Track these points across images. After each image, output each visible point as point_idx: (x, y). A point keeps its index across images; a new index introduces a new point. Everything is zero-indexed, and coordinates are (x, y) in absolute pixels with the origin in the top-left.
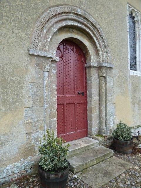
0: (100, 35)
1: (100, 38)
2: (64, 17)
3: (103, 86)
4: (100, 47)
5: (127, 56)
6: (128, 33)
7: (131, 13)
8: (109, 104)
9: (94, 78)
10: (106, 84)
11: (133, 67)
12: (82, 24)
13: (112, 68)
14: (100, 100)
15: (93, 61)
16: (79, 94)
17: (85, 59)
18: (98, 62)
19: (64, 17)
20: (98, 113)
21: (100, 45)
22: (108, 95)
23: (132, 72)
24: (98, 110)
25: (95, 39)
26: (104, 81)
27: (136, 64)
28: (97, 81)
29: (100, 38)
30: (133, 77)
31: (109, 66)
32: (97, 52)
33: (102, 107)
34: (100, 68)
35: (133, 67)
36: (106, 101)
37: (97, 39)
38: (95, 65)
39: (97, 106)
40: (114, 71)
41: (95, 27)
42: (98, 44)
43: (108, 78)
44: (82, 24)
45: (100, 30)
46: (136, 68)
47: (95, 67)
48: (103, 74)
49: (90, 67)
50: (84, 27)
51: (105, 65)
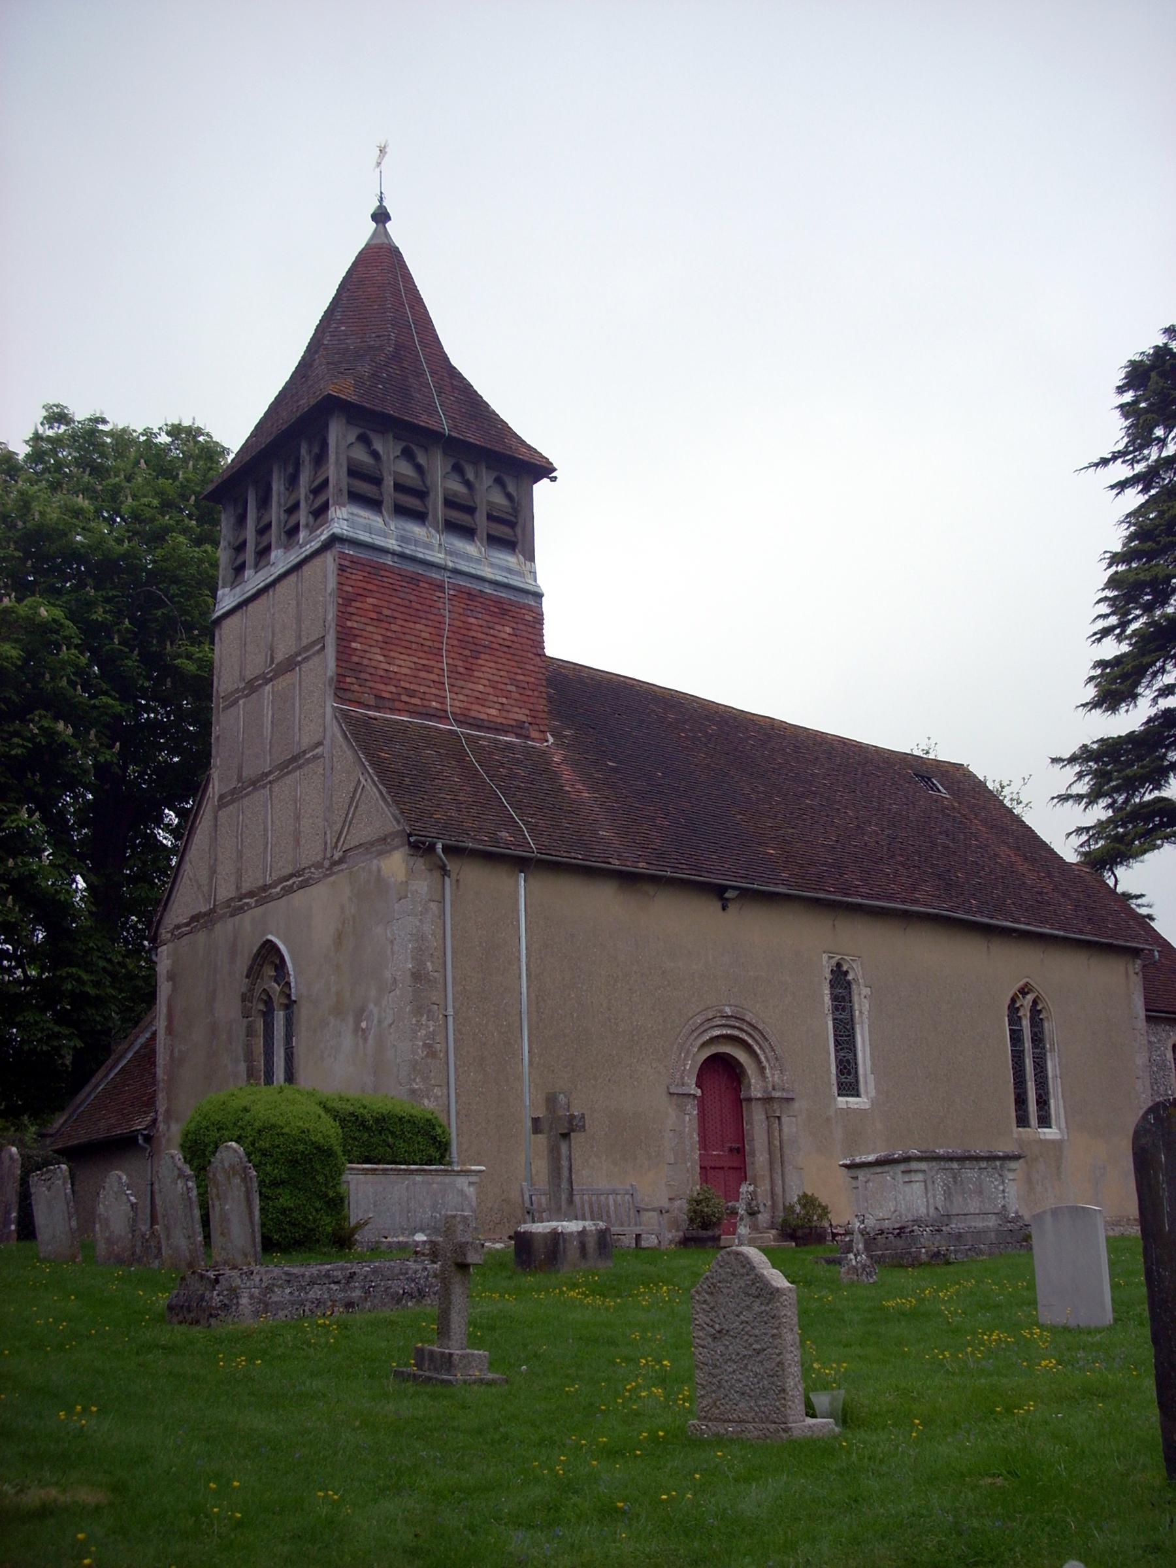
0: (767, 1040)
1: (765, 1045)
2: (707, 1026)
3: (777, 1134)
4: (768, 1060)
5: (829, 1070)
6: (830, 1017)
7: (839, 965)
8: (789, 1168)
9: (757, 1119)
10: (780, 1131)
11: (849, 1087)
12: (734, 1027)
13: (793, 1099)
14: (771, 1163)
15: (755, 1087)
16: (731, 1150)
17: (740, 1083)
18: (765, 1090)
19: (707, 1026)
20: (769, 1188)
21: (766, 1057)
22: (787, 1151)
23: (842, 1101)
24: (767, 1181)
25: (756, 1048)
26: (776, 1125)
27: (857, 1082)
28: (765, 1125)
29: (765, 1045)
30: (848, 1111)
31: (785, 1095)
32: (762, 1069)
33: (775, 1175)
34: (768, 1100)
35: (849, 1087)
36: (782, 1162)
37: (761, 1048)
38: (759, 1095)
39: (767, 1173)
40: (796, 1105)
41: (755, 1028)
42: (762, 1058)
43: (784, 1119)
44: (734, 1027)
45: (767, 1030)
46: (858, 1090)
47: (759, 1099)
48: (774, 1111)
49: (749, 1100)
50: (736, 1033)
51: (777, 1094)
